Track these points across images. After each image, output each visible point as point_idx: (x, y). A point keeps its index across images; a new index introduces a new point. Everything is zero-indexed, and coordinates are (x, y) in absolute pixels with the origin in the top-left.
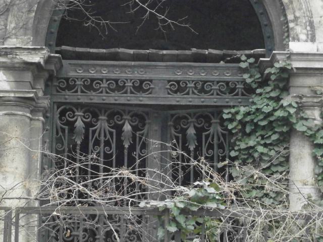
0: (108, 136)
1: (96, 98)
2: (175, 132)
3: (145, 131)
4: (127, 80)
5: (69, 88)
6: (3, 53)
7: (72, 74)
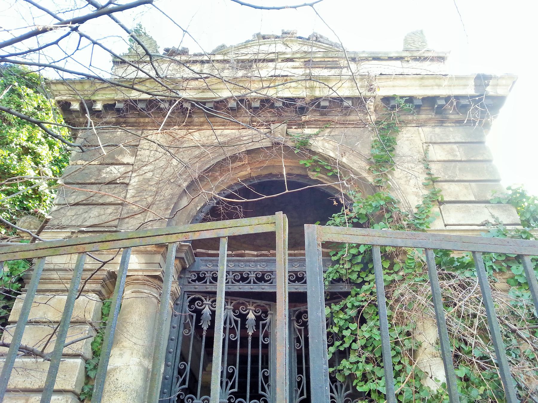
0: (233, 324)
4: (250, 272)
5: (200, 279)
7: (203, 268)
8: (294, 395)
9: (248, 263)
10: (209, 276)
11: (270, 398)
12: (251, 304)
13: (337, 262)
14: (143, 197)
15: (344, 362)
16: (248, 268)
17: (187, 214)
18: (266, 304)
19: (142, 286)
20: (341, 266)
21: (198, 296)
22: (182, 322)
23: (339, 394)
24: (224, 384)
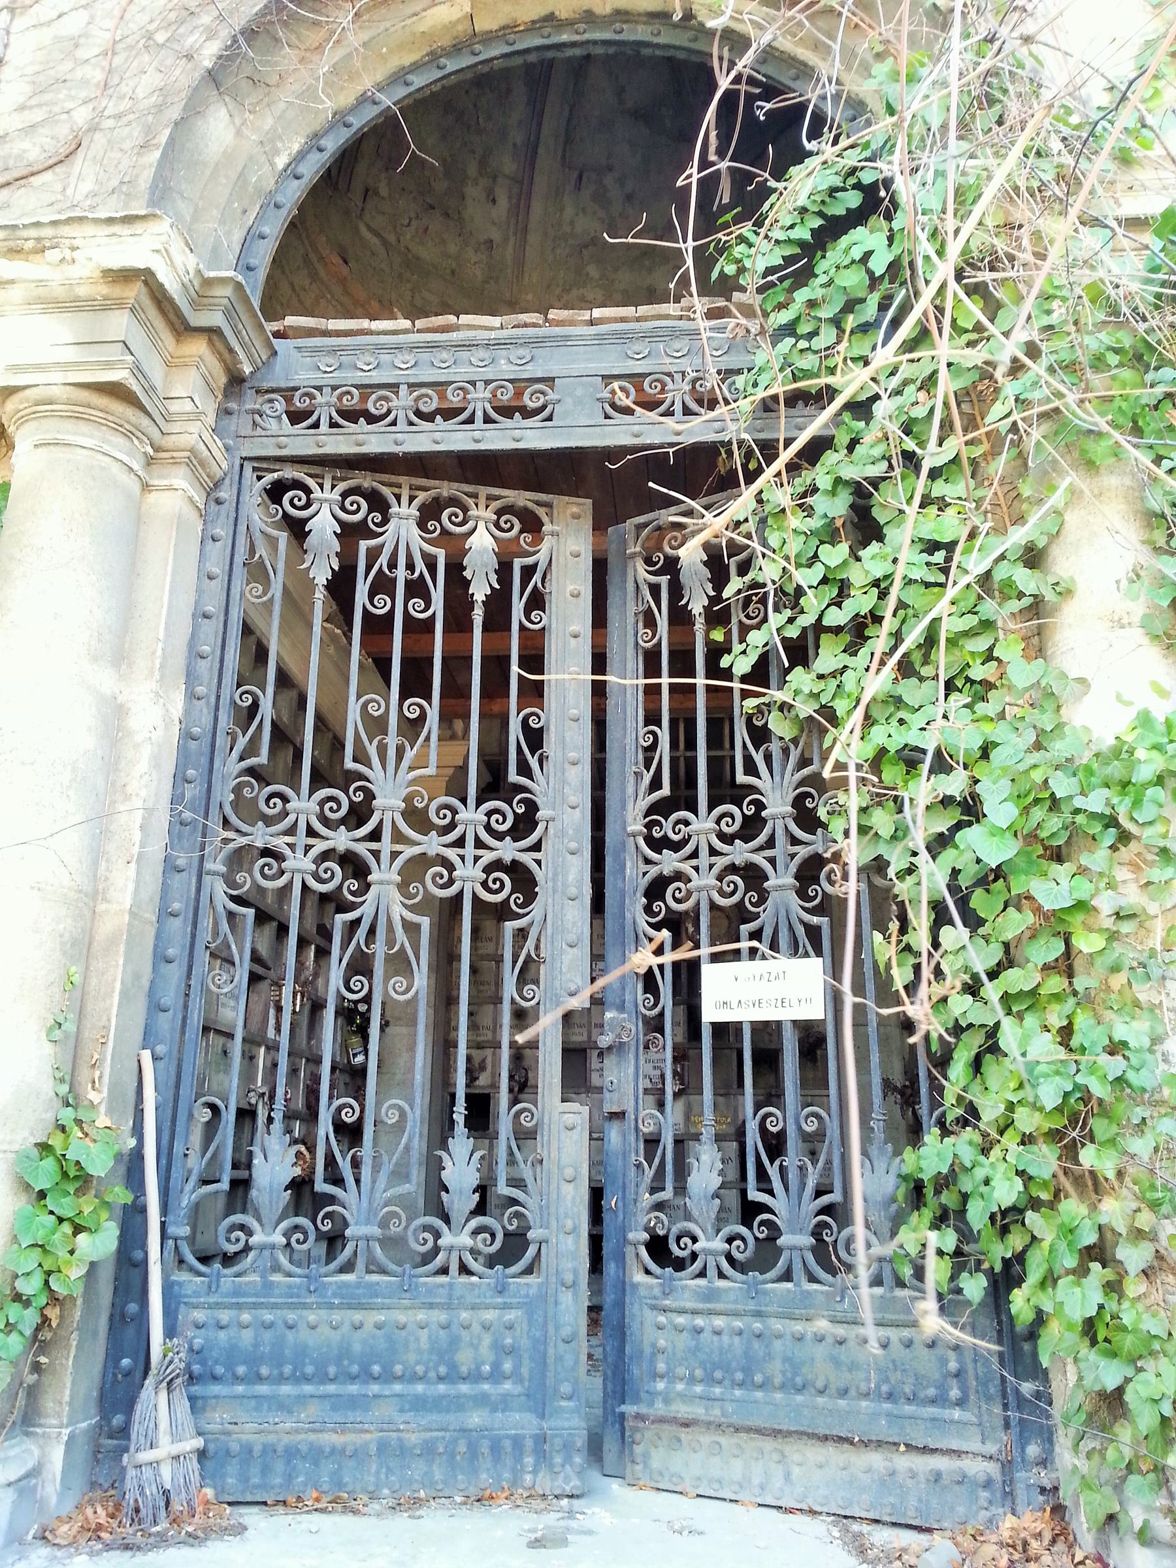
1: (373, 438)
2: (649, 572)
3: (542, 557)
4: (473, 383)
6: (30, 245)
7: (303, 377)
8: (630, 790)
9: (465, 355)
10: (328, 404)
11: (546, 795)
12: (482, 501)
13: (789, 329)
14: (56, 109)
15: (800, 678)
16: (462, 373)
17: (234, 176)
18: (538, 503)
19: (69, 425)
20: (803, 344)
21: (289, 473)
22: (239, 559)
23: (777, 778)
24: (391, 753)
